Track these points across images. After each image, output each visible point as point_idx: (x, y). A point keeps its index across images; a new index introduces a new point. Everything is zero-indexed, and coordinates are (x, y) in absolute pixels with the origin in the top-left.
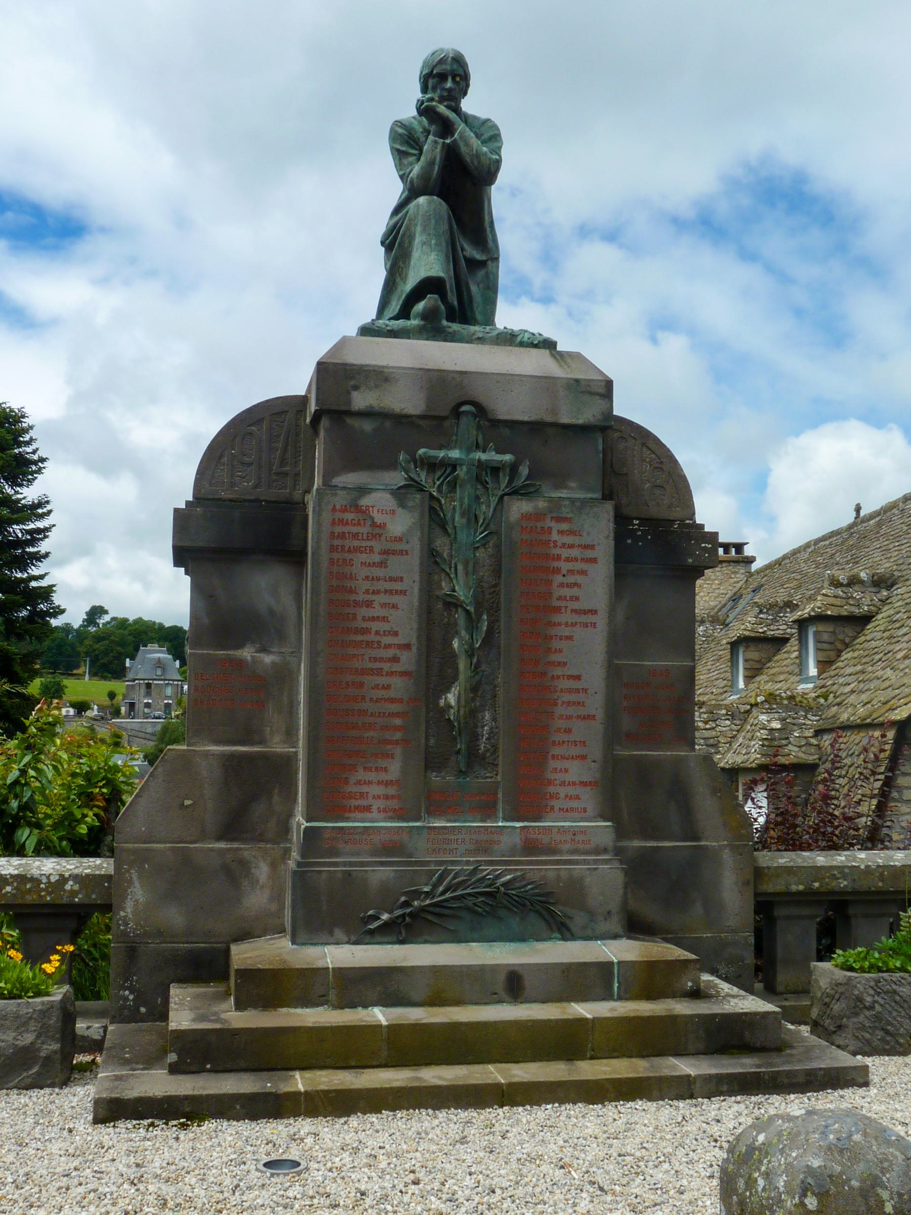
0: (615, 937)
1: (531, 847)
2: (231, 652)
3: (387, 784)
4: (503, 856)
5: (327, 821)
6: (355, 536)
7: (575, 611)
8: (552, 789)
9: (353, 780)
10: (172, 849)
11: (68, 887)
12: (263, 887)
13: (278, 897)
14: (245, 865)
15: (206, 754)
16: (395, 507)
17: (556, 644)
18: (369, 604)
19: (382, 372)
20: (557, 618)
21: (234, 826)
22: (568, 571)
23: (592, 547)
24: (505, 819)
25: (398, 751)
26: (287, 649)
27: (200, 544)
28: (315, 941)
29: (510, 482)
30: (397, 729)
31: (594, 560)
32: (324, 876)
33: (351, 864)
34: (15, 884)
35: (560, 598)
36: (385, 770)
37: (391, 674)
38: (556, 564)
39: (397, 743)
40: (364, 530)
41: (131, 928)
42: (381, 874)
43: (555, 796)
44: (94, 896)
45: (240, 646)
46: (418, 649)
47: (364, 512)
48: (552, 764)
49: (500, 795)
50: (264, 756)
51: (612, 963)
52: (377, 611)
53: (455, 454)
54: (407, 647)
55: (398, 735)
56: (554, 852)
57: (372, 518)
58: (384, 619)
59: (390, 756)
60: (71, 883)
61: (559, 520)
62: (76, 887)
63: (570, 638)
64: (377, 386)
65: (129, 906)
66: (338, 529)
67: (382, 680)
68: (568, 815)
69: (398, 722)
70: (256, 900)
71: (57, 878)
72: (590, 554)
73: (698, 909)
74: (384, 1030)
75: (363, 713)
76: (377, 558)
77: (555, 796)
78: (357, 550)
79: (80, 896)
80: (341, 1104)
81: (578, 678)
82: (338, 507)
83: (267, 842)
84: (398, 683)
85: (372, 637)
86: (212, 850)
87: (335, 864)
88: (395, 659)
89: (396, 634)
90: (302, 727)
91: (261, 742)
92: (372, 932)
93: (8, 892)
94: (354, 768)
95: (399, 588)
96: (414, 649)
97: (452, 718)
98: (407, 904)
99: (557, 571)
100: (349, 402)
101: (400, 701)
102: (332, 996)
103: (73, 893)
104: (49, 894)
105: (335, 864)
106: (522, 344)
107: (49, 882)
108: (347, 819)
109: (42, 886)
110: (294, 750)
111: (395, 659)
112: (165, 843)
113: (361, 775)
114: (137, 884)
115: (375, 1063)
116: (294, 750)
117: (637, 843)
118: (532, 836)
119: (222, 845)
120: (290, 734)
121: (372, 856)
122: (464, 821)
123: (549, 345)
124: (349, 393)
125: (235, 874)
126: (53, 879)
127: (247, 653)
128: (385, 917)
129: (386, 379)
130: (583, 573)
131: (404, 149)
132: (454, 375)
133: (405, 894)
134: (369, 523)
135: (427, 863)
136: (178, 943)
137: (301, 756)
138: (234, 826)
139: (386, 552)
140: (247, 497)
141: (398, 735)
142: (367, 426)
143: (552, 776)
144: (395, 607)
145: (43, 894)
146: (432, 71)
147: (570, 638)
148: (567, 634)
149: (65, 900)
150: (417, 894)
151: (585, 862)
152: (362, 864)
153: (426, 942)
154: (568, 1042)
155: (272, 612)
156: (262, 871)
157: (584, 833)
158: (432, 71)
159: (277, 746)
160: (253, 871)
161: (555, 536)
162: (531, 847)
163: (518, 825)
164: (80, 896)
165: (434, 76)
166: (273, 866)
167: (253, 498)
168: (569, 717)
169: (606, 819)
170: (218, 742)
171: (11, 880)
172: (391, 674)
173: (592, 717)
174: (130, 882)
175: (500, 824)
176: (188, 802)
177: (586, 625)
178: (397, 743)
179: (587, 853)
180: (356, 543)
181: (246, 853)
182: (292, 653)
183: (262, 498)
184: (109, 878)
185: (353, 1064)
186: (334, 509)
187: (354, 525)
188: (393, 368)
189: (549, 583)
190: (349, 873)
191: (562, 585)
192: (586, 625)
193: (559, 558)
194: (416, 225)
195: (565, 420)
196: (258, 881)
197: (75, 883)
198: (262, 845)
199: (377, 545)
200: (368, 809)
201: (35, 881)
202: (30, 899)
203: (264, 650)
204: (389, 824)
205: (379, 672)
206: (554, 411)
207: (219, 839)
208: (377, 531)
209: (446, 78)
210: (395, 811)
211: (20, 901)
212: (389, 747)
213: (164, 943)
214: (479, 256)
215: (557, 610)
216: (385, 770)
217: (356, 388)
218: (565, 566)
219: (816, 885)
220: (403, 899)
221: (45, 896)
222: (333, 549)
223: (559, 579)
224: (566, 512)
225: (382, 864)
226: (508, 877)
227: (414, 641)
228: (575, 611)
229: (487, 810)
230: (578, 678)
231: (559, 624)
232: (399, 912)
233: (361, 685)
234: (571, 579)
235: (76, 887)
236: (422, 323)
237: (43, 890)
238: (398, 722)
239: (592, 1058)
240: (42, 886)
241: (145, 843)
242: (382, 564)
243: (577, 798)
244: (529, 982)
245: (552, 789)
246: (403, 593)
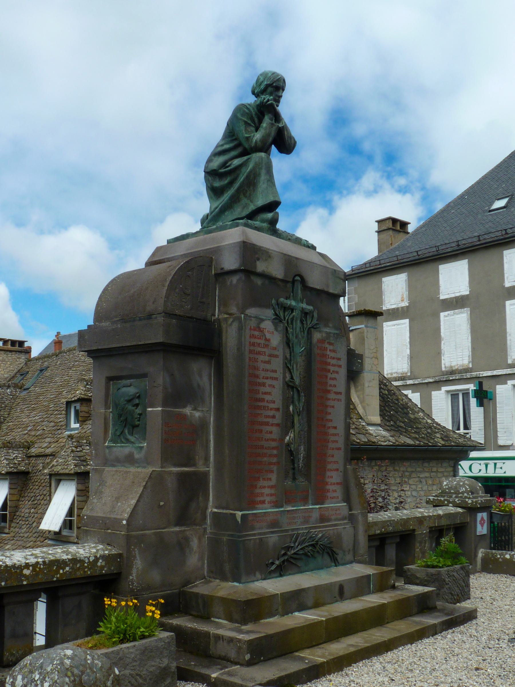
2: (181, 410)
3: (271, 487)
4: (313, 524)
5: (249, 510)
6: (259, 345)
8: (328, 487)
9: (258, 486)
10: (155, 534)
11: (99, 564)
12: (195, 553)
13: (201, 559)
14: (187, 540)
15: (170, 473)
16: (274, 331)
17: (330, 410)
18: (264, 385)
19: (268, 252)
21: (183, 518)
22: (333, 371)
24: (313, 504)
25: (275, 468)
26: (205, 409)
27: (174, 342)
28: (249, 580)
30: (276, 456)
32: (252, 541)
33: (260, 534)
34: (71, 565)
36: (270, 479)
37: (272, 425)
39: (275, 464)
40: (262, 342)
41: (135, 586)
42: (273, 539)
43: (328, 491)
44: (112, 568)
45: (185, 407)
46: (282, 411)
47: (261, 330)
48: (328, 474)
49: (310, 491)
50: (195, 473)
51: (370, 575)
52: (267, 389)
53: (293, 303)
54: (278, 410)
55: (275, 460)
56: (329, 520)
57: (265, 335)
58: (269, 394)
59: (272, 472)
60: (100, 561)
62: (103, 564)
63: (333, 407)
64: (266, 260)
65: (134, 572)
66: (253, 340)
68: (334, 500)
69: (275, 452)
70: (193, 561)
71: (93, 558)
74: (324, 622)
75: (262, 447)
76: (267, 358)
77: (328, 491)
78: (259, 353)
79: (105, 569)
80: (339, 664)
81: (335, 428)
82: (252, 328)
83: (197, 525)
84: (275, 429)
85: (265, 404)
86: (173, 532)
87: (254, 535)
88: (274, 417)
89: (274, 402)
90: (211, 455)
91: (194, 465)
92: (271, 572)
93: (67, 571)
94: (258, 479)
95: (275, 376)
96: (281, 410)
97: (292, 449)
98: (285, 554)
100: (255, 267)
102: (280, 610)
103: (102, 567)
104: (89, 569)
105: (254, 535)
106: (304, 245)
107: (89, 562)
108: (256, 509)
109: (86, 565)
110: (208, 469)
111: (274, 417)
112: (151, 530)
113: (262, 483)
114: (138, 557)
115: (322, 642)
116: (208, 469)
118: (323, 513)
119: (177, 529)
120: (207, 459)
121: (267, 528)
122: (298, 507)
123: (314, 248)
124: (256, 262)
125: (183, 545)
126: (91, 559)
127: (187, 411)
128: (277, 562)
129: (270, 257)
130: (337, 372)
131: (249, 122)
132: (294, 259)
133: (283, 548)
134: (264, 338)
135: (287, 531)
136: (157, 592)
137: (211, 472)
138: (183, 518)
139: (270, 356)
140: (187, 315)
141: (275, 460)
142: (259, 282)
144: (274, 387)
145: (86, 570)
146: (273, 83)
147: (333, 407)
148: (332, 405)
149: (98, 573)
150: (288, 548)
151: (341, 525)
152: (265, 534)
153: (290, 574)
154: (377, 617)
155: (199, 386)
156: (195, 543)
157: (339, 509)
158: (273, 83)
159: (202, 468)
160: (191, 543)
161: (328, 353)
162: (323, 519)
163: (317, 507)
164: (105, 569)
165: (273, 87)
166: (200, 539)
167: (190, 316)
168: (333, 449)
169: (345, 502)
170: (175, 465)
171: (68, 563)
172: (272, 425)
174: (135, 557)
175: (311, 507)
176: (162, 503)
178: (275, 464)
179: (340, 520)
180: (259, 349)
181: (188, 533)
182: (207, 411)
183: (194, 316)
184: (120, 555)
185: (314, 644)
186: (251, 329)
187: (258, 338)
188: (272, 250)
190: (261, 539)
194: (261, 169)
195: (331, 291)
196: (193, 549)
197: (103, 561)
198: (194, 527)
199: (267, 351)
200: (263, 502)
201: (82, 561)
202: (79, 574)
203: (195, 409)
204: (273, 510)
205: (267, 424)
206: (328, 286)
207: (176, 525)
208: (267, 343)
210: (274, 502)
211: (74, 577)
212: (272, 466)
213: (151, 593)
216: (270, 479)
217: (258, 259)
218: (332, 369)
220: (283, 552)
221: (87, 572)
222: (251, 352)
224: (332, 340)
225: (272, 532)
226: (320, 535)
227: (281, 407)
229: (305, 500)
230: (335, 428)
231: (330, 399)
232: (282, 559)
233: (261, 431)
234: (334, 376)
235: (103, 564)
236: (269, 226)
237: (86, 567)
238: (275, 452)
240: (86, 565)
241: (142, 531)
242: (269, 362)
245: (328, 487)
246: (276, 379)
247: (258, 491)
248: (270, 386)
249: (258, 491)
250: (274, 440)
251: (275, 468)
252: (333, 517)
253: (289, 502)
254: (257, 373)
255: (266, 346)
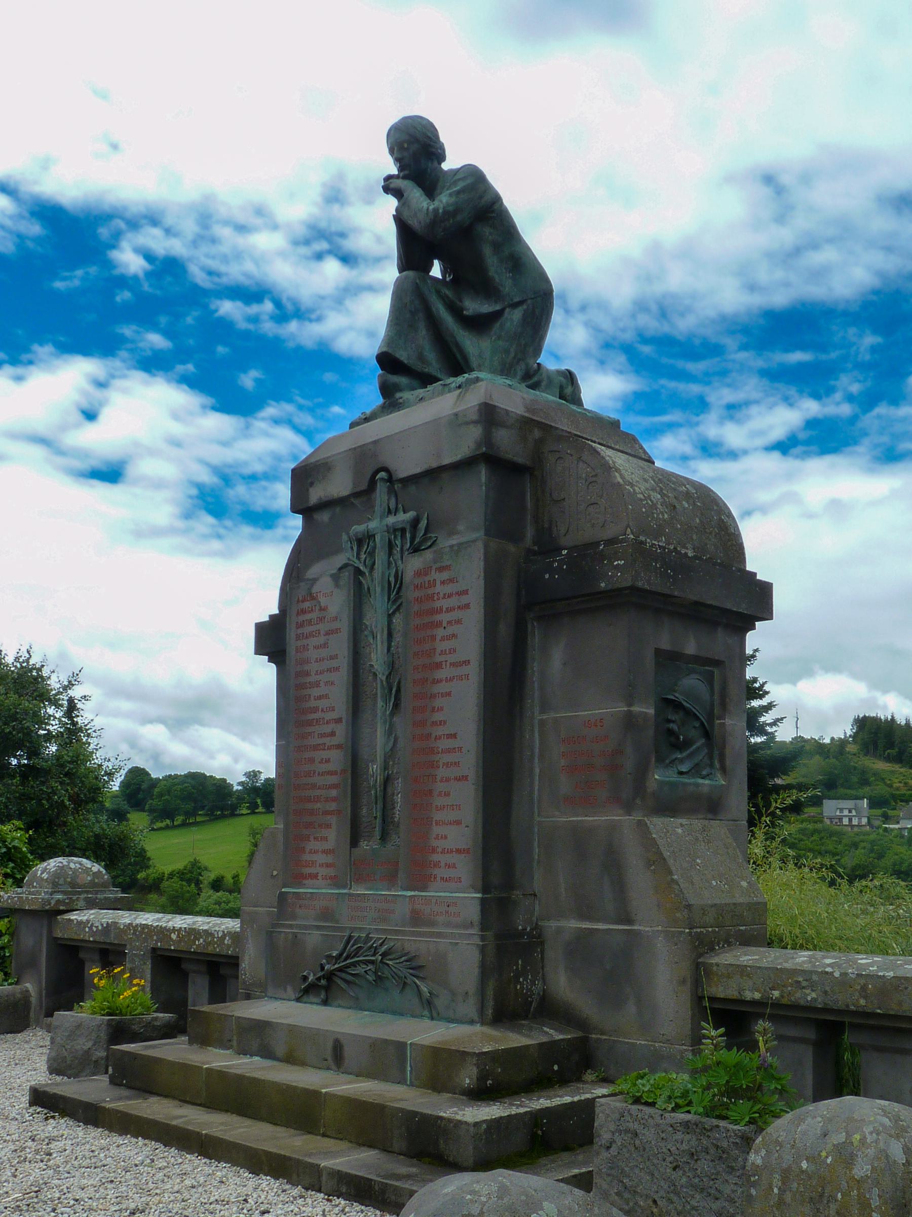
0: (472, 1022)
1: (416, 918)
4: (397, 925)
7: (453, 665)
8: (435, 857)
9: (307, 850)
18: (317, 684)
20: (441, 674)
23: (466, 592)
25: (333, 820)
29: (412, 542)
30: (334, 799)
31: (467, 606)
32: (283, 935)
35: (443, 653)
36: (325, 839)
38: (438, 617)
43: (437, 865)
48: (437, 830)
54: (339, 720)
56: (432, 924)
57: (319, 602)
58: (326, 696)
59: (329, 826)
61: (441, 569)
67: (325, 754)
72: (464, 600)
73: (631, 1008)
75: (314, 786)
76: (322, 640)
77: (437, 865)
81: (453, 736)
87: (291, 926)
88: (333, 734)
89: (333, 709)
99: (439, 624)
101: (335, 773)
105: (291, 926)
111: (333, 734)
113: (312, 845)
117: (574, 924)
122: (377, 890)
130: (459, 622)
141: (333, 806)
143: (434, 843)
147: (449, 694)
157: (455, 904)
162: (416, 918)
168: (448, 780)
172: (330, 748)
173: (465, 778)
176: (275, 873)
177: (460, 678)
179: (457, 926)
187: (310, 612)
189: (433, 638)
190: (295, 935)
191: (442, 639)
192: (460, 678)
193: (440, 611)
199: (323, 627)
200: (315, 876)
209: (416, 149)
210: (331, 878)
212: (329, 817)
214: (486, 308)
215: (439, 666)
216: (326, 839)
218: (444, 617)
219: (776, 994)
222: (298, 637)
223: (440, 633)
228: (453, 665)
229: (391, 879)
230: (453, 736)
231: (441, 681)
234: (450, 630)
238: (334, 793)
239: (324, 1135)
242: (325, 645)
243: (454, 866)
244: (349, 1052)
245: (435, 857)
247: (307, 857)
248: (326, 683)
249: (307, 857)
250: (335, 773)
251: (333, 820)
252: (440, 919)
253: (359, 879)
254: (306, 668)
255: (321, 619)
